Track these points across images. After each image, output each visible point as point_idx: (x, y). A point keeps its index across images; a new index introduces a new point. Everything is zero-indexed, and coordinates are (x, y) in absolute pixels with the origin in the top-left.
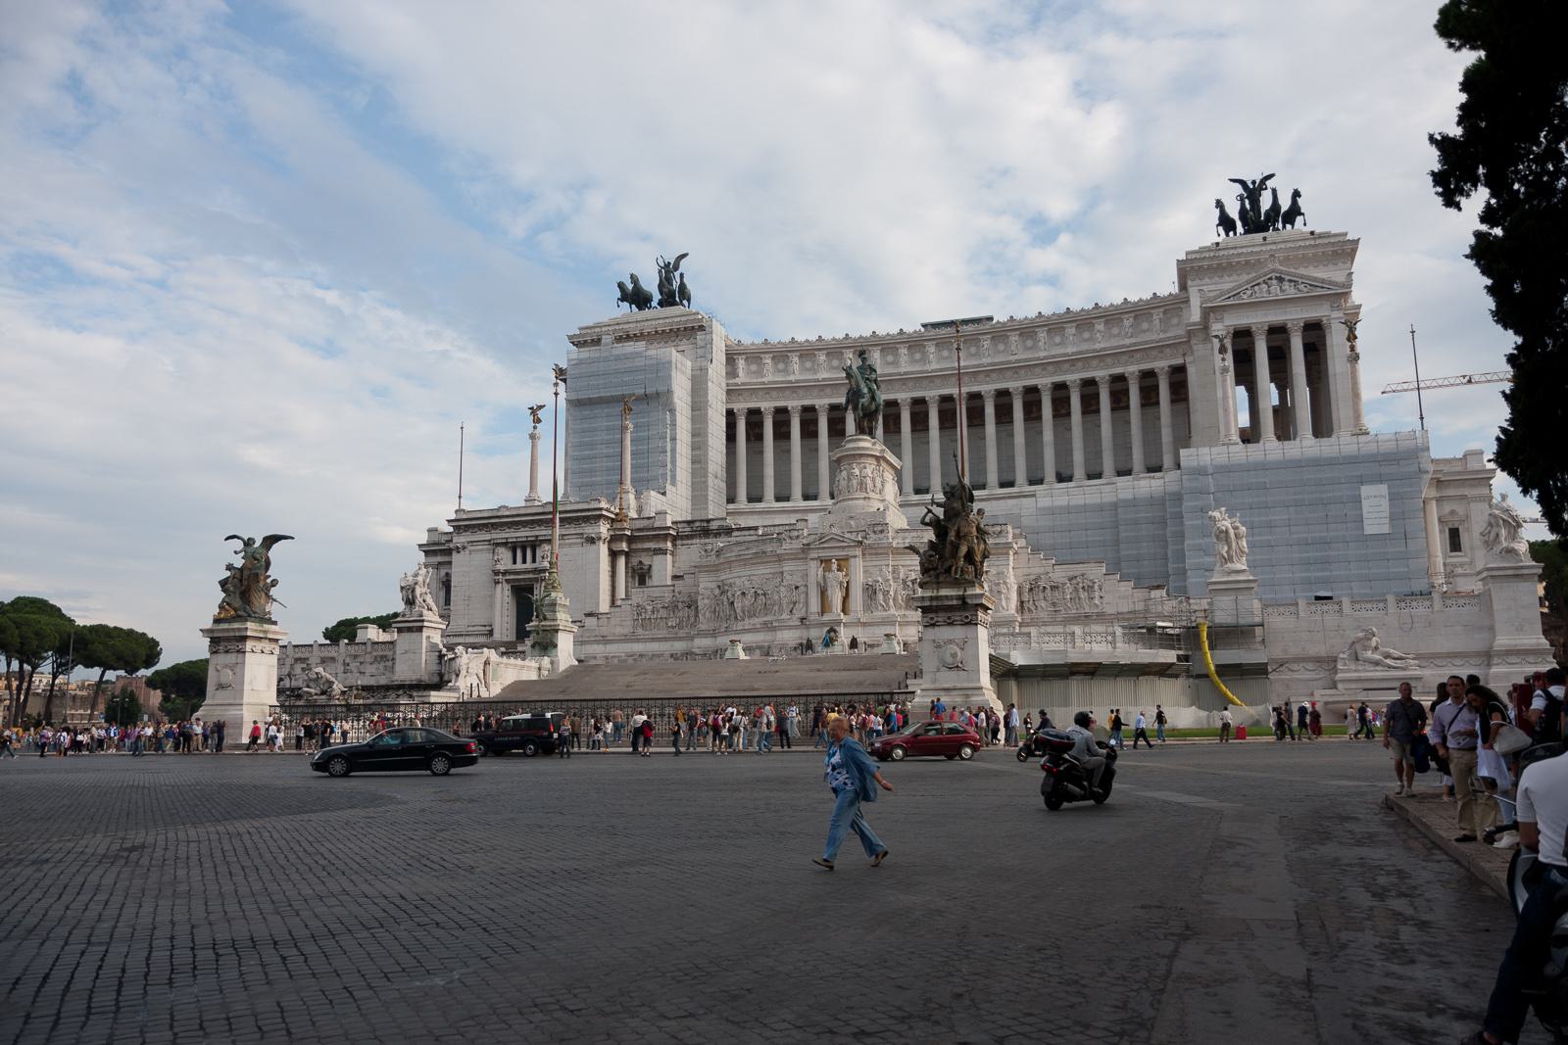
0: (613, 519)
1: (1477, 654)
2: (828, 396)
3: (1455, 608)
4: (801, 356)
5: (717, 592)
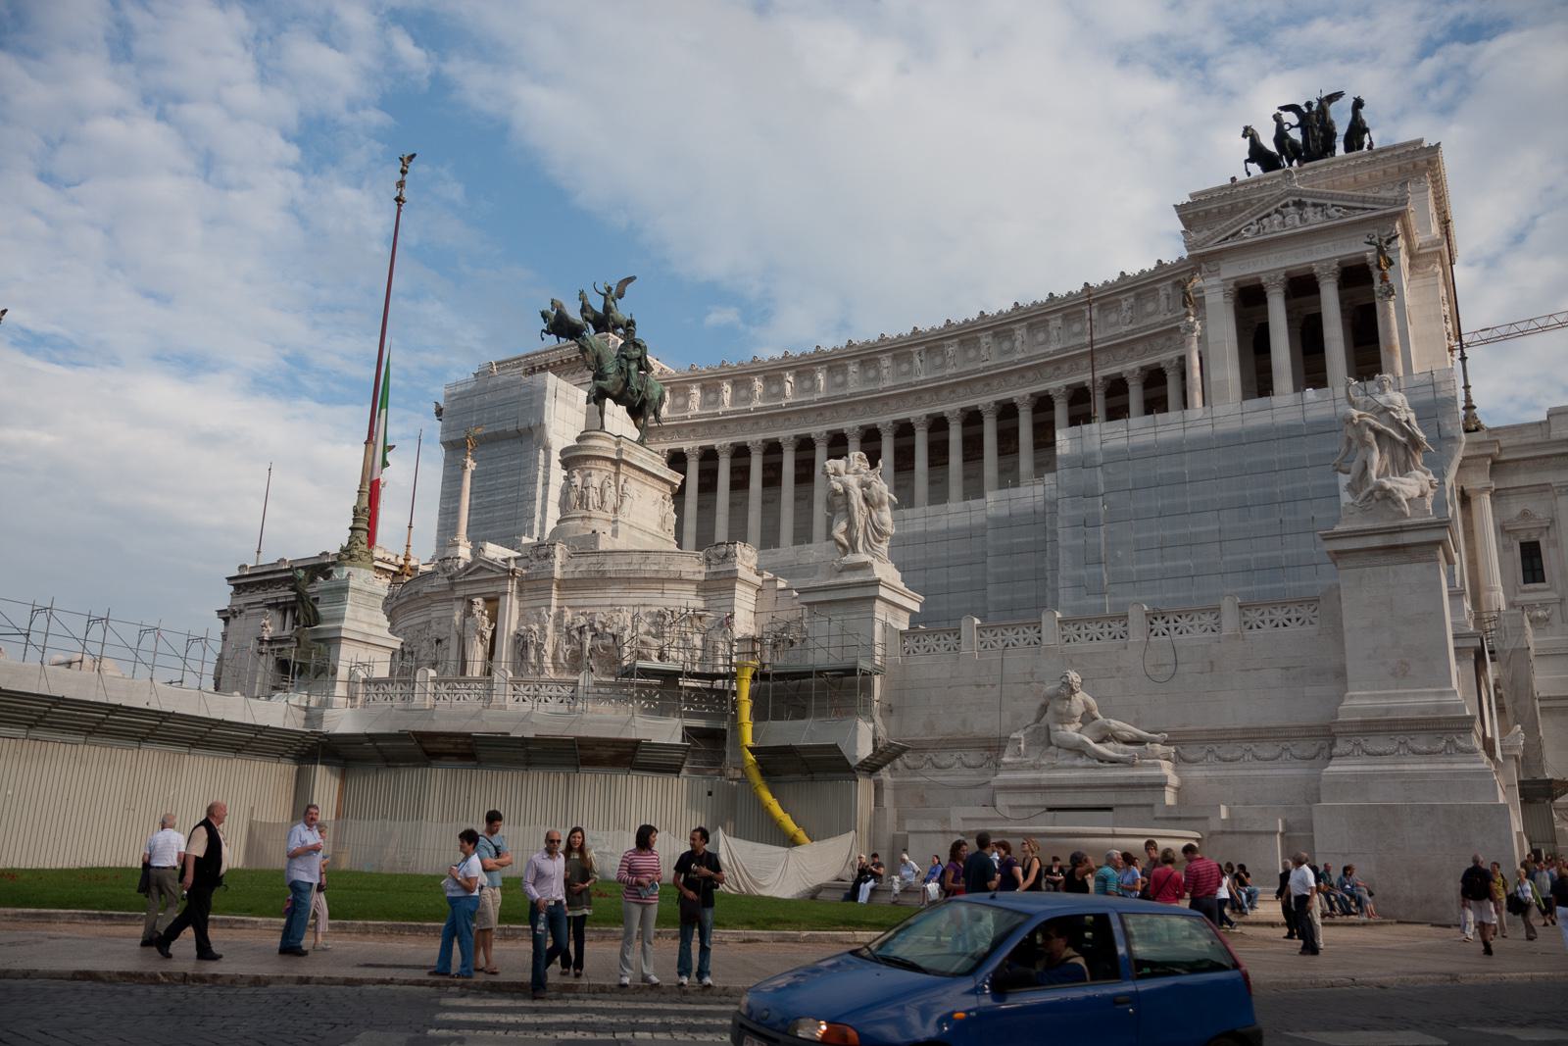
0: (394, 572)
1: (1309, 732)
2: (766, 430)
3: (1267, 627)
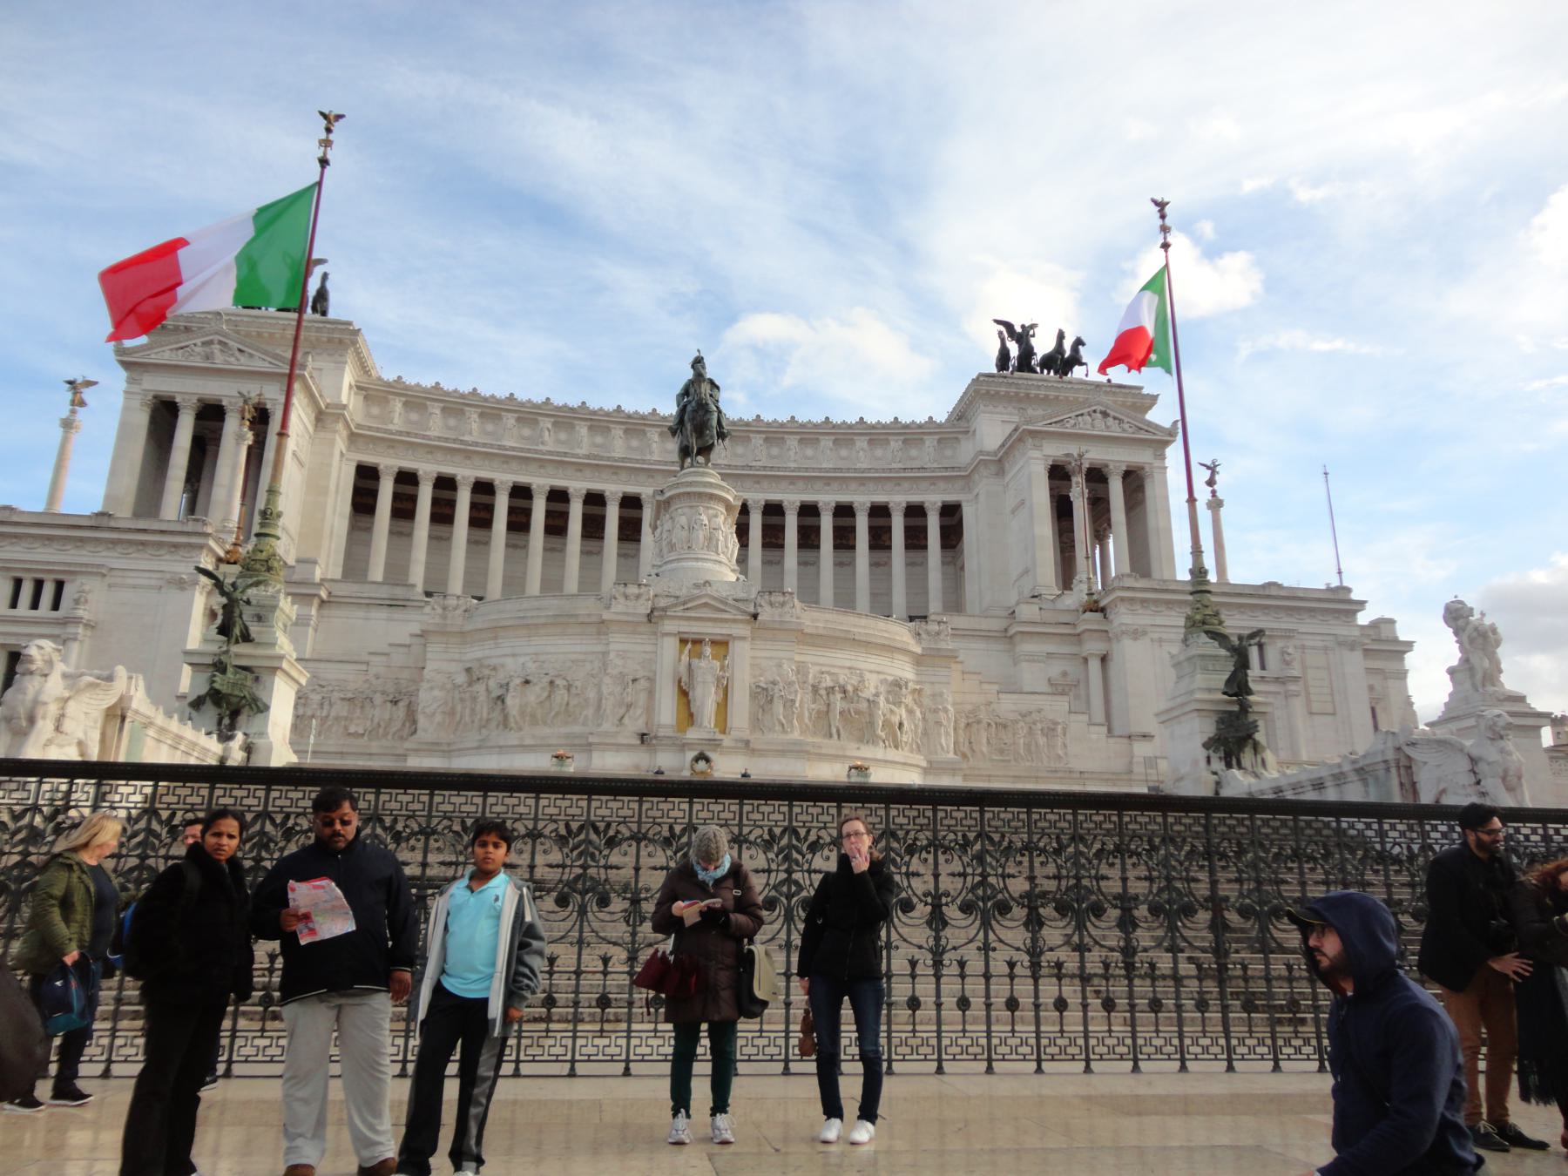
0: (220, 560)
5: (461, 679)
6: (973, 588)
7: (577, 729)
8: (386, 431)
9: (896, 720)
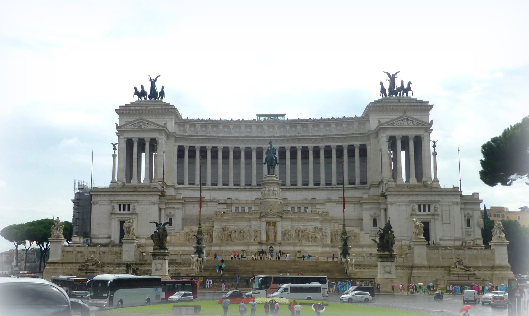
4: (212, 126)
5: (221, 230)
6: (369, 174)
7: (246, 241)
8: (185, 136)
9: (314, 236)
